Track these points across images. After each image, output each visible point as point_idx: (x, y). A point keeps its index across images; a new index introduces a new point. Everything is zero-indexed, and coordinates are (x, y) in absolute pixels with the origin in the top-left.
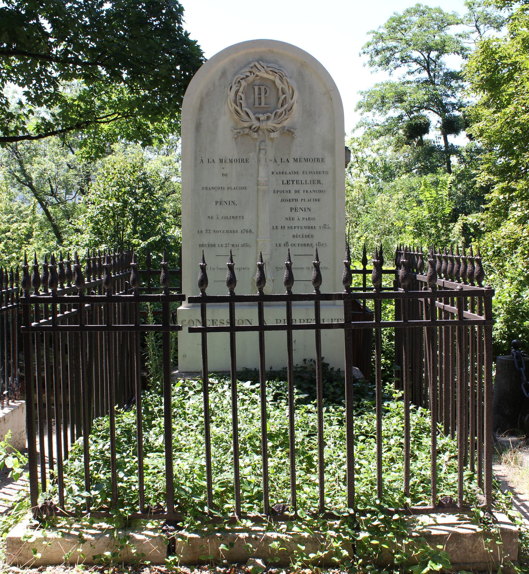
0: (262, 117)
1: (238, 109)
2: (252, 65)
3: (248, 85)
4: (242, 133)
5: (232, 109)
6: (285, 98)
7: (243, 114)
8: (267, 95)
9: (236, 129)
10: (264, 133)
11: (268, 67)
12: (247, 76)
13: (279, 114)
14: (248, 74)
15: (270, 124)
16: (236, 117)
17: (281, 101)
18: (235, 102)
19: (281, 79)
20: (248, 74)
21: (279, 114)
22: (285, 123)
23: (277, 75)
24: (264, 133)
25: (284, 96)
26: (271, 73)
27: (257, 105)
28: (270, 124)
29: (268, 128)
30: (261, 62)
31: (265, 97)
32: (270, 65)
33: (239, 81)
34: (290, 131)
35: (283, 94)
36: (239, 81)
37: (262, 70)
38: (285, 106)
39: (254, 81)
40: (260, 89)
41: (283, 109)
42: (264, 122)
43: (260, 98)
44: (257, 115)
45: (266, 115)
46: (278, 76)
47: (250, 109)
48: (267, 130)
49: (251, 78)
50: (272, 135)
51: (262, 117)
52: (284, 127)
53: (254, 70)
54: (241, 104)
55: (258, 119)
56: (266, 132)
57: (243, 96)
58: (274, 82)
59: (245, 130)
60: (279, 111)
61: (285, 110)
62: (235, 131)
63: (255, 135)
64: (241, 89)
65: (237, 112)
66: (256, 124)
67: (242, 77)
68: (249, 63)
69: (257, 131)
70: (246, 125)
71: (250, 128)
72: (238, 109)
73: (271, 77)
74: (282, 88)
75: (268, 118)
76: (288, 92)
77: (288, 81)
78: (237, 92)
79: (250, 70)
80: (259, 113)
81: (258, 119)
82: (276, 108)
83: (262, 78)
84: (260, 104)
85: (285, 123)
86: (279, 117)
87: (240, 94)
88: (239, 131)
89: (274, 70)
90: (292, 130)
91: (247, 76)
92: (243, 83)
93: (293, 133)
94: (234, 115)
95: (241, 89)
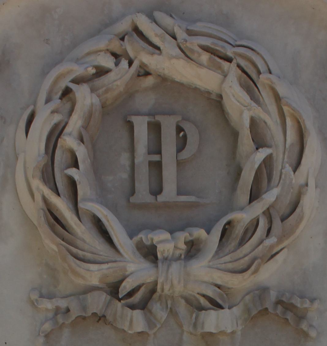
0: (167, 244)
1: (61, 205)
2: (124, 26)
3: (106, 109)
4: (75, 312)
5: (34, 210)
6: (268, 162)
7: (82, 231)
8: (185, 154)
9: (50, 297)
10: (173, 313)
11: (190, 33)
12: (101, 72)
13: (239, 230)
14: (107, 62)
15: (205, 273)
16: (51, 244)
17: (248, 176)
18: (48, 175)
19: (249, 82)
20: (107, 62)
21: (239, 230)
22: (268, 274)
23: (232, 69)
24: (173, 313)
25: (261, 155)
26: (205, 57)
27: (143, 193)
28: (205, 273)
29: (194, 290)
30: (158, 15)
31: (180, 164)
32: (198, 27)
33: (67, 92)
34: (288, 307)
35: (259, 142)
36: (67, 92)
37: (168, 47)
38: (270, 197)
39: (129, 95)
40: (155, 129)
41: (258, 209)
42: (175, 267)
43: (157, 167)
44: (146, 237)
45: (182, 237)
46: (232, 69)
47: (114, 209)
48: (188, 301)
49: (119, 77)
50: (212, 321)
51: (167, 244)
52: (262, 291)
53: (131, 47)
54: (73, 184)
55: (150, 253)
56: (182, 308)
57: (81, 152)
58: (217, 102)
59: (90, 297)
60: (243, 218)
61: (268, 213)
62: (48, 305)
63: (137, 321)
64: (75, 123)
65: (55, 220)
66: (137, 272)
67: (79, 71)
68: (110, 22)
69: (143, 305)
70: (94, 275)
71: (114, 290)
72: (61, 205)
73: (204, 78)
74: (254, 123)
75: (193, 249)
76: (282, 140)
77: (282, 90)
78: (56, 134)
79: (116, 46)
80: (154, 228)
81: (150, 253)
82: (230, 207)
83: (164, 81)
84: (157, 191)
85: (268, 274)
86: (242, 242)
87: (69, 141)
88: (63, 304)
89: (220, 47)
90: (297, 302)
91: (101, 72)
92: (85, 97)
93: (301, 317)
94: (44, 231)
95: (75, 123)
